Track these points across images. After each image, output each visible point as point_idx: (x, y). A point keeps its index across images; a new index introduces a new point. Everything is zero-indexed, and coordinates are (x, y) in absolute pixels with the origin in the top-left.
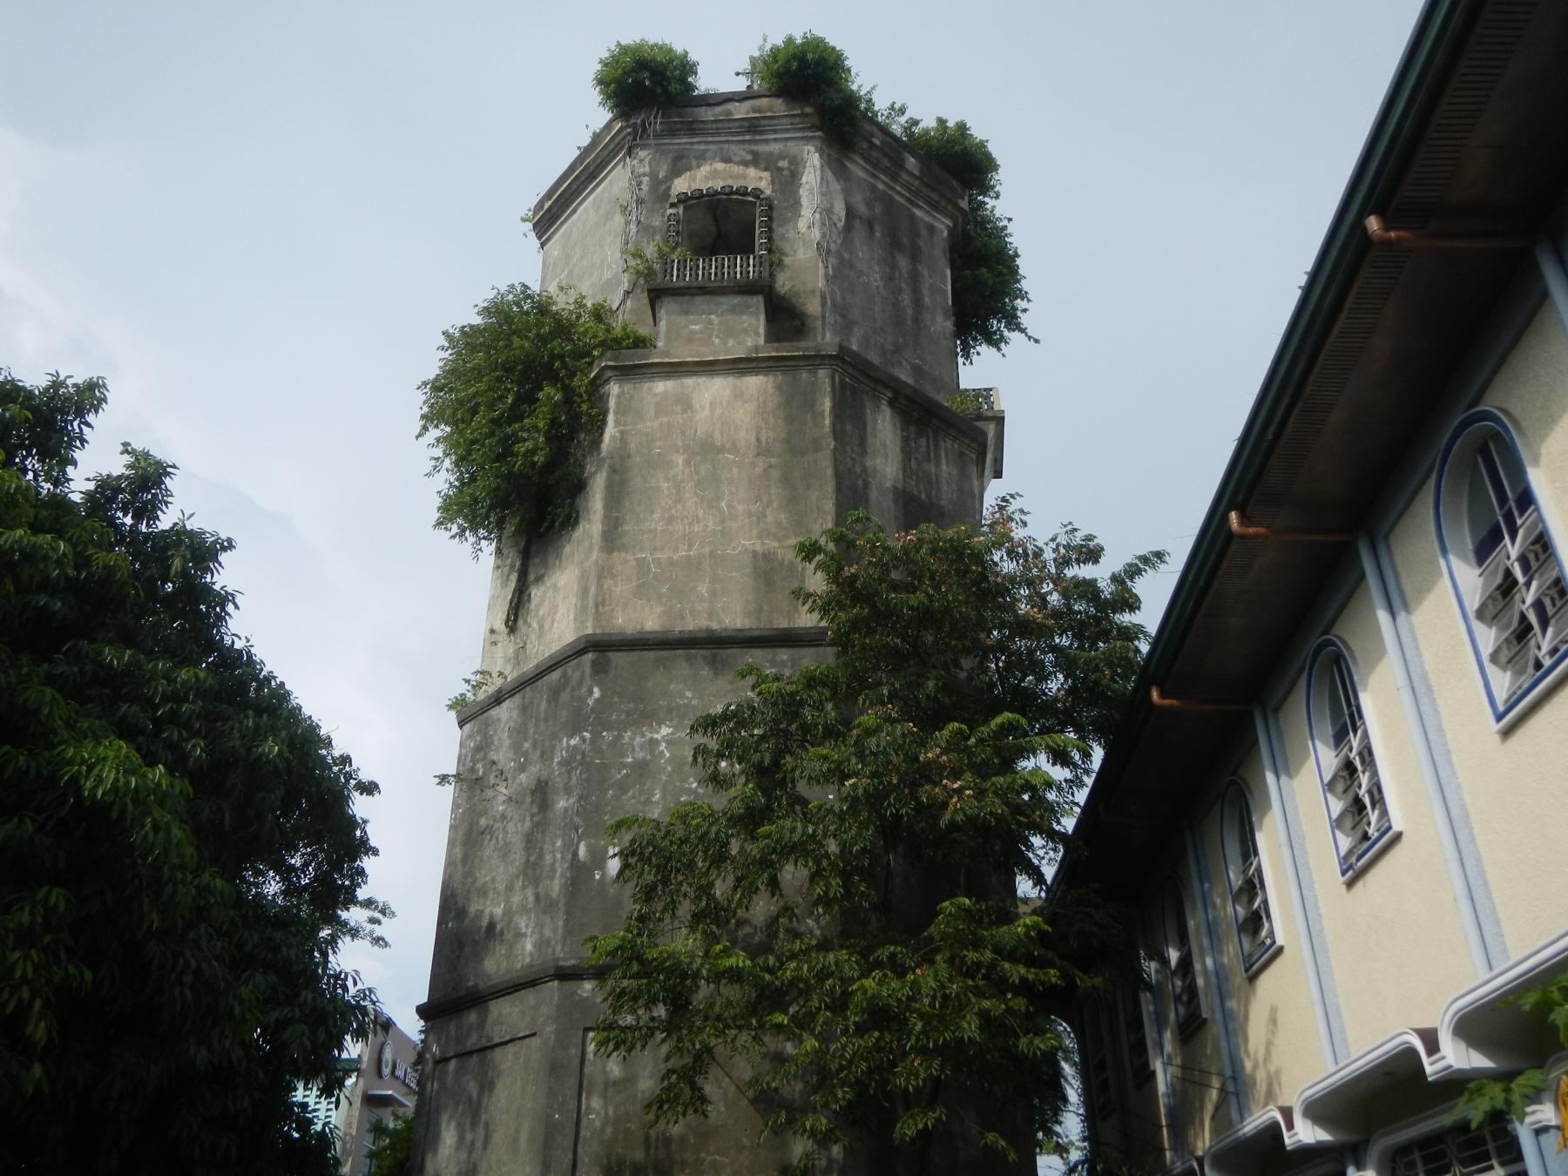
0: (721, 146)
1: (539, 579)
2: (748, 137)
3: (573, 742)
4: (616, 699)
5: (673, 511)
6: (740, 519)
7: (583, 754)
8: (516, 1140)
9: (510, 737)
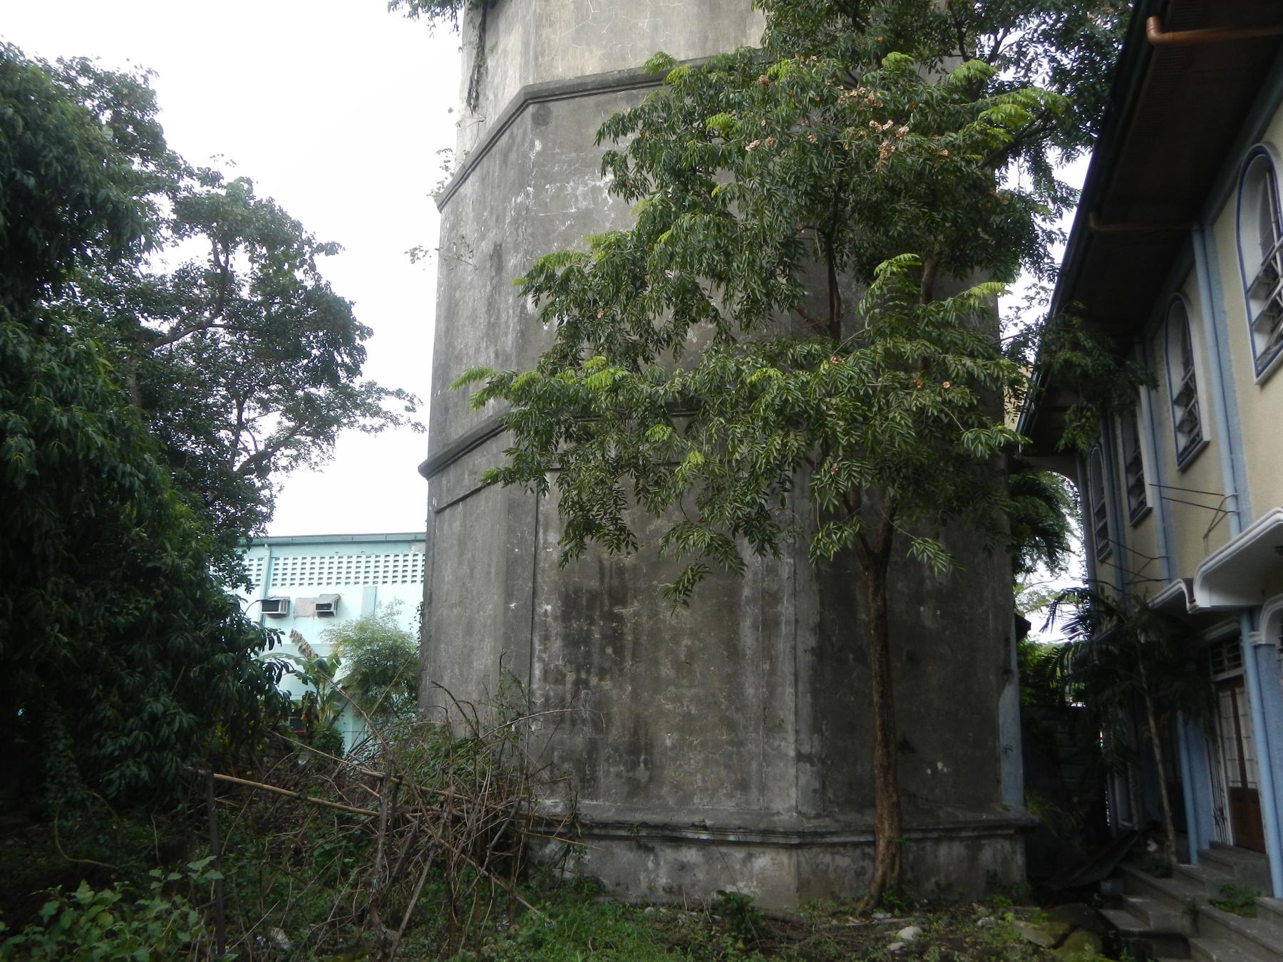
1: (493, 49)
3: (519, 200)
4: (558, 150)
7: (527, 209)
8: (489, 573)
9: (473, 210)
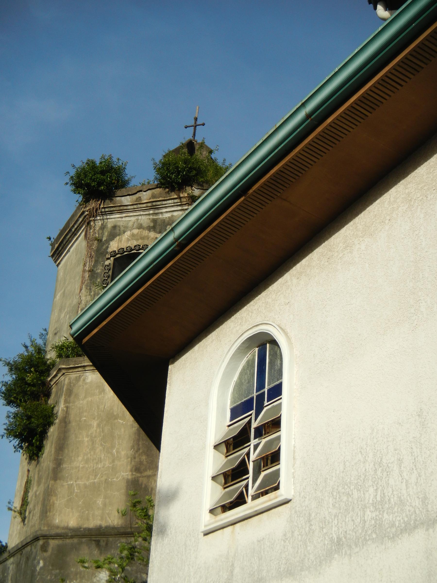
0: (136, 218)
2: (151, 212)
5: (89, 455)
6: (122, 459)
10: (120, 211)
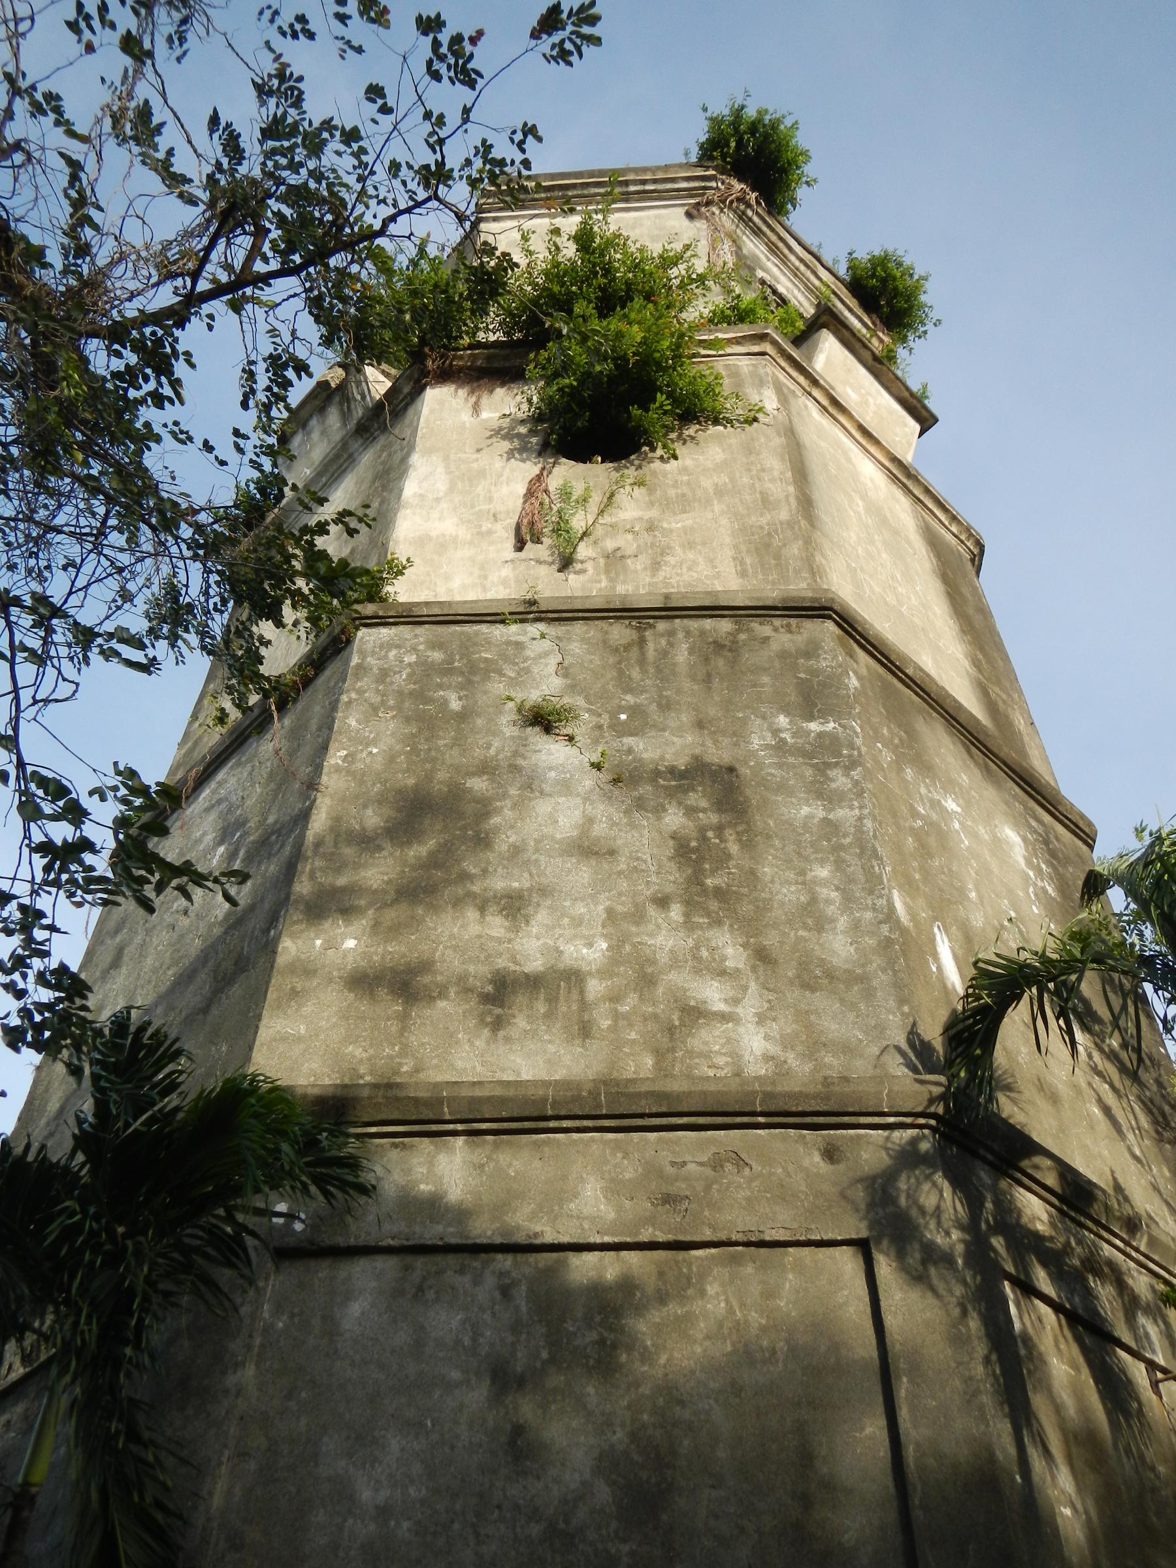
10: (773, 249)
